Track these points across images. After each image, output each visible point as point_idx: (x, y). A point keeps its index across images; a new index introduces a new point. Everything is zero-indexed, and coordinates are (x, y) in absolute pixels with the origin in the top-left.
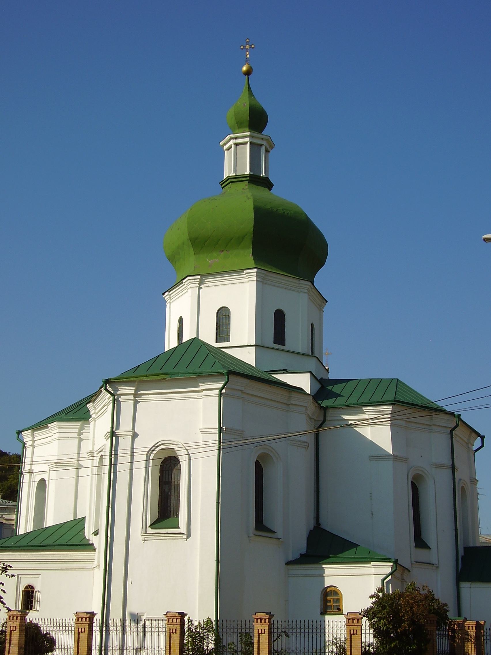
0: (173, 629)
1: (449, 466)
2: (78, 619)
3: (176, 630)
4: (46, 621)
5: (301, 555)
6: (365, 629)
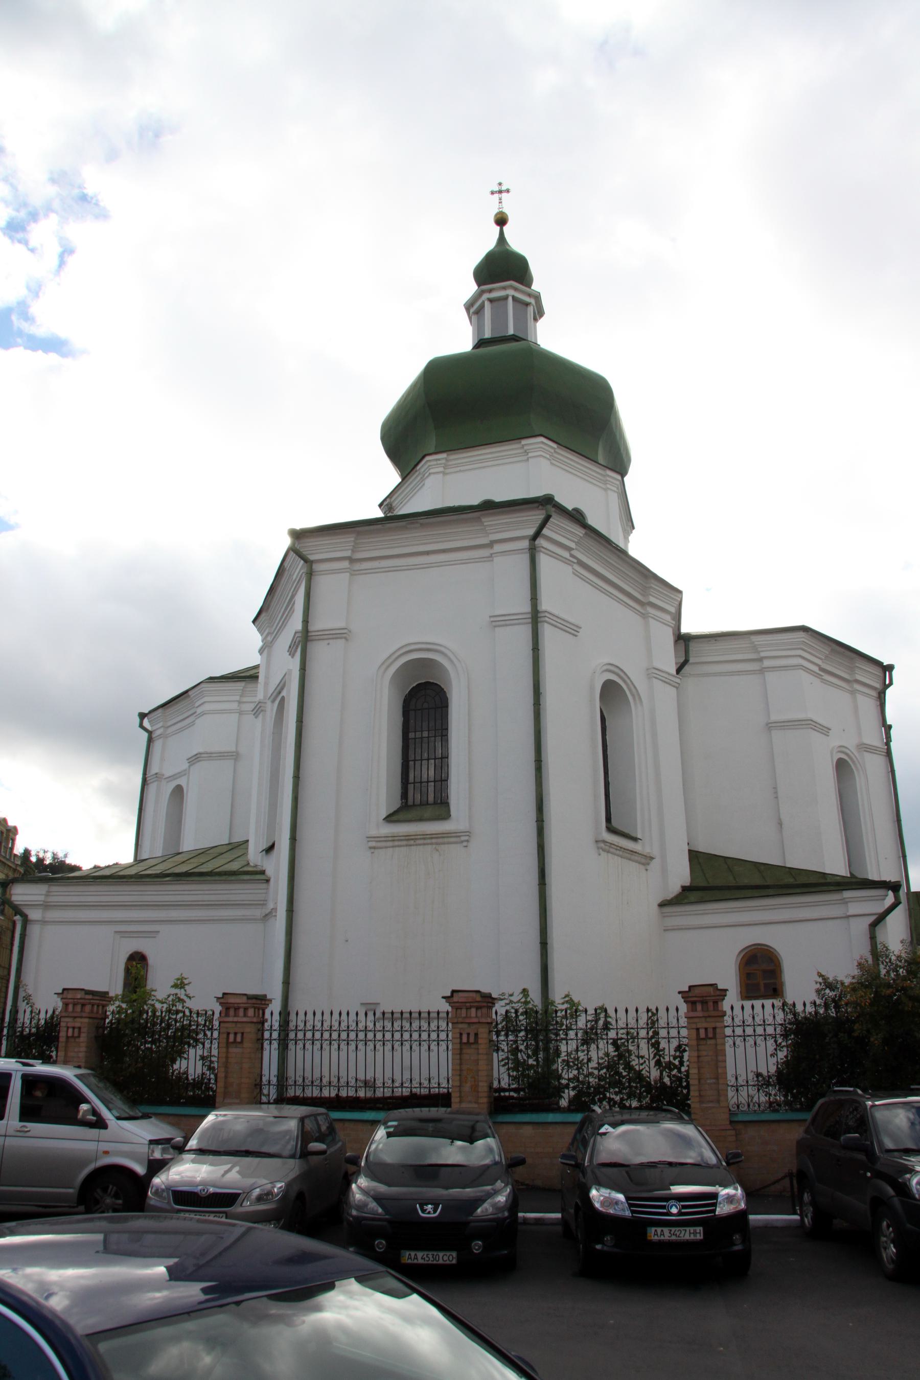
0: (468, 1034)
2: (227, 1009)
3: (476, 1035)
5: (684, 889)
6: (755, 1036)
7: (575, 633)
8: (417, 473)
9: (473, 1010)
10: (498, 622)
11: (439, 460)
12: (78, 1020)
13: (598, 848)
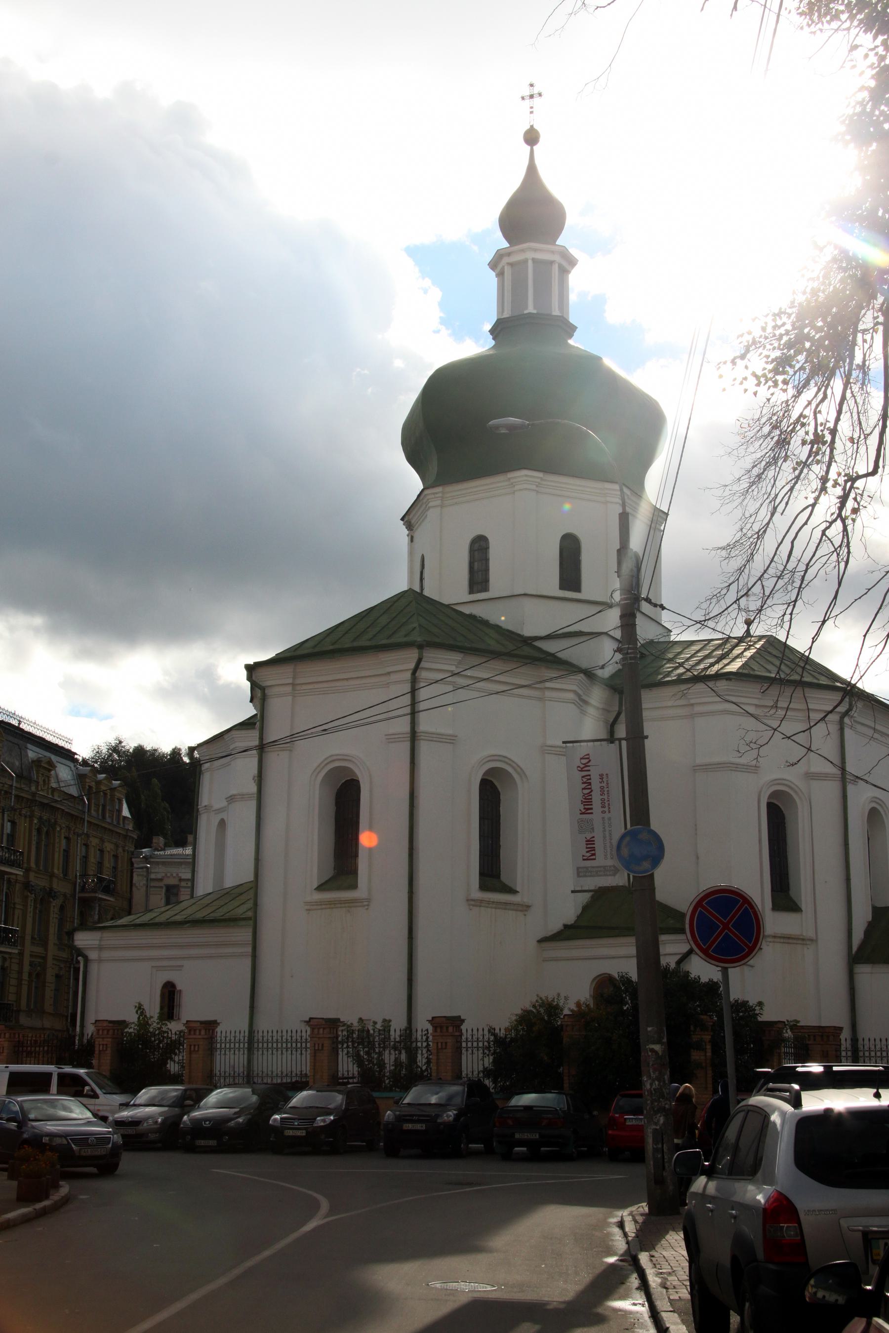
0: (319, 1044)
1: (836, 776)
3: (323, 1045)
4: (237, 1034)
5: (566, 927)
7: (452, 741)
8: (421, 503)
9: (321, 1030)
10: (391, 739)
11: (436, 493)
12: (105, 1039)
13: (469, 905)
